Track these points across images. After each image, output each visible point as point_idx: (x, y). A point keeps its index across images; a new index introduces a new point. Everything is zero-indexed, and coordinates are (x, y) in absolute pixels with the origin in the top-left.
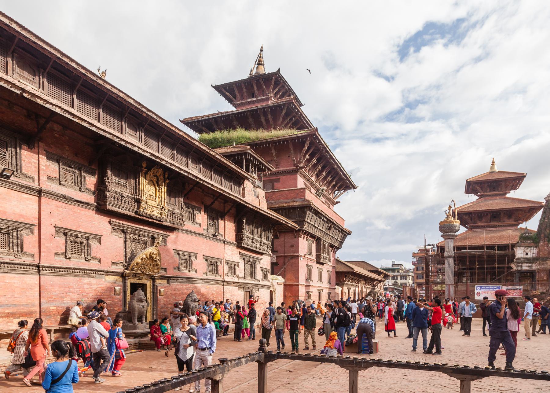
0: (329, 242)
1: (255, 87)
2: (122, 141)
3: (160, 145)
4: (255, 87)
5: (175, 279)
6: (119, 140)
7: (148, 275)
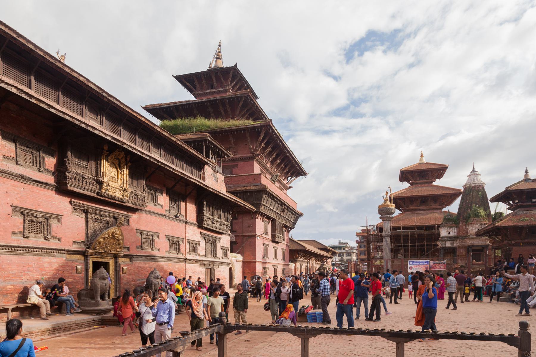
1: (214, 79)
2: (82, 124)
3: (122, 130)
4: (214, 79)
5: (138, 257)
6: (79, 122)
7: (110, 253)
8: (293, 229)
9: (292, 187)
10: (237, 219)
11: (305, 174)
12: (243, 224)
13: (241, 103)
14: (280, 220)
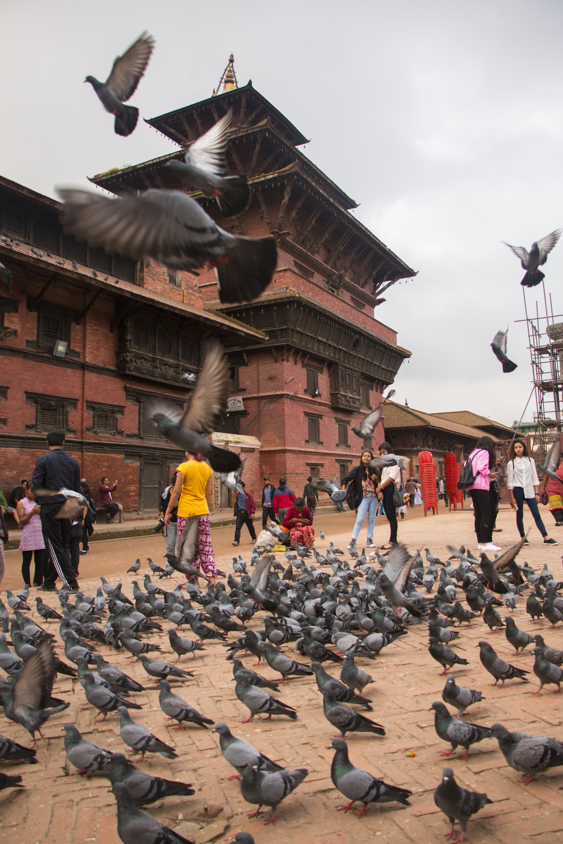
0: (361, 370)
8: (391, 384)
9: (384, 300)
10: (247, 366)
11: (409, 273)
12: (258, 374)
13: (257, 145)
14: (349, 364)
